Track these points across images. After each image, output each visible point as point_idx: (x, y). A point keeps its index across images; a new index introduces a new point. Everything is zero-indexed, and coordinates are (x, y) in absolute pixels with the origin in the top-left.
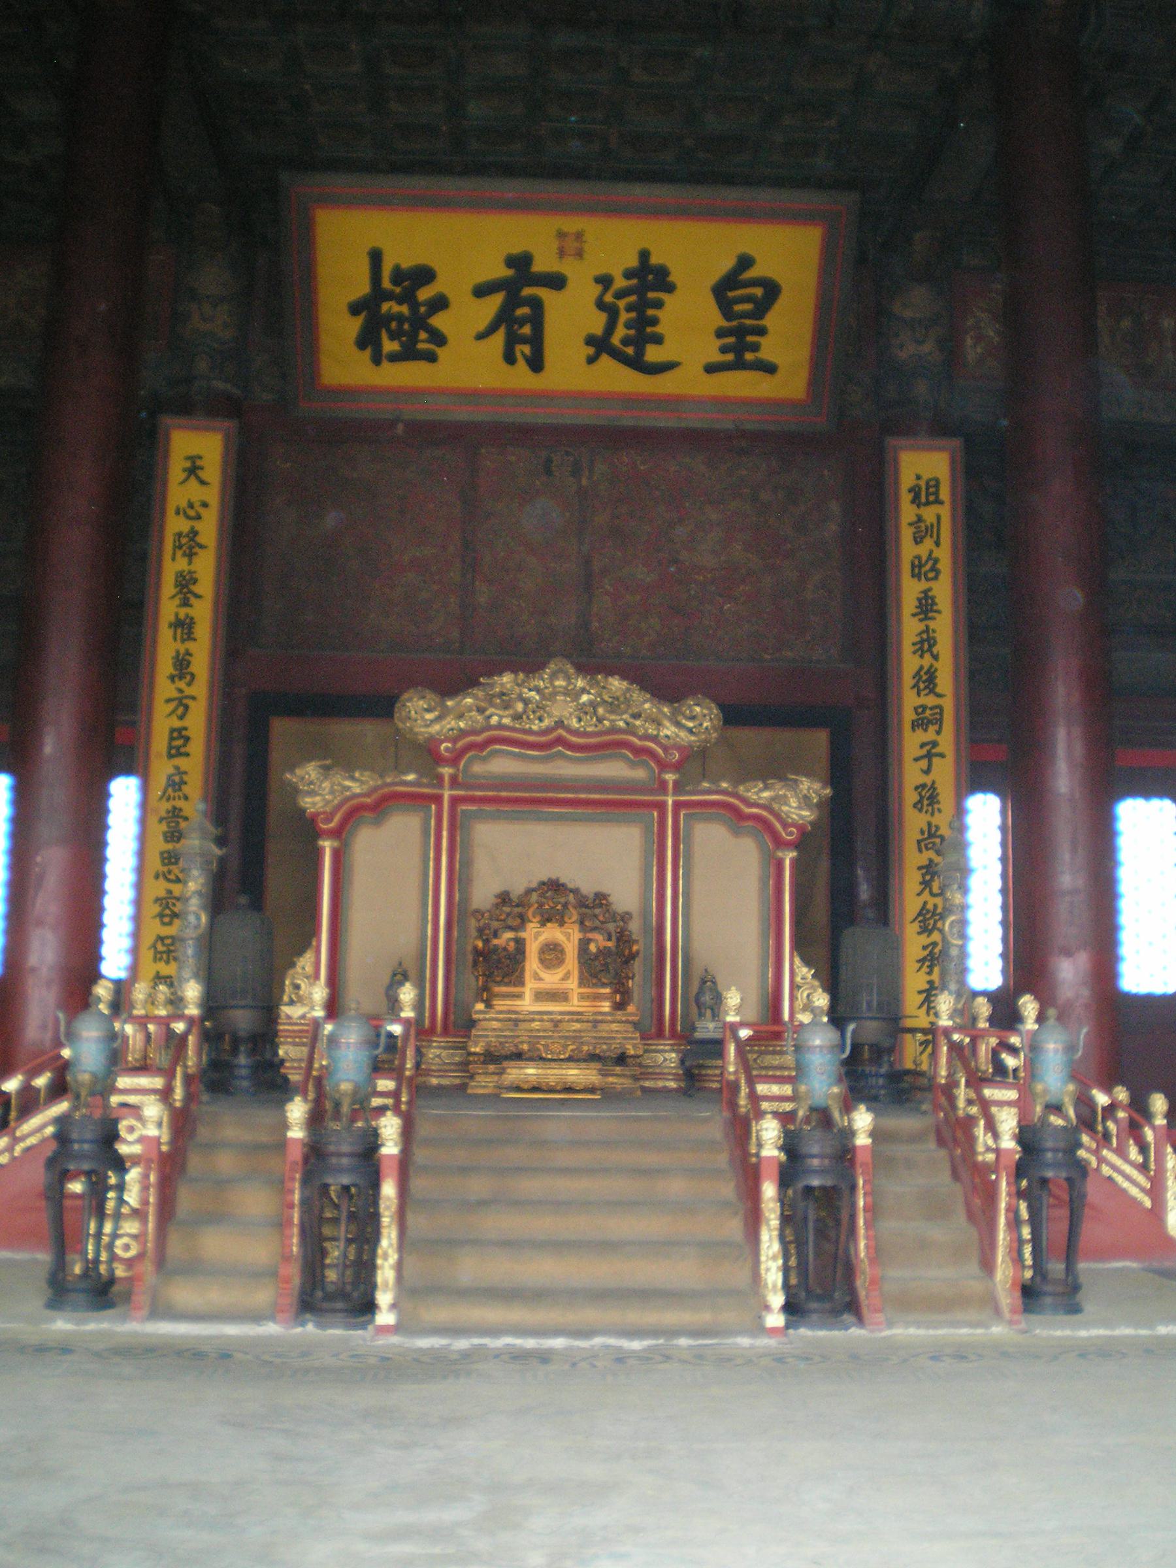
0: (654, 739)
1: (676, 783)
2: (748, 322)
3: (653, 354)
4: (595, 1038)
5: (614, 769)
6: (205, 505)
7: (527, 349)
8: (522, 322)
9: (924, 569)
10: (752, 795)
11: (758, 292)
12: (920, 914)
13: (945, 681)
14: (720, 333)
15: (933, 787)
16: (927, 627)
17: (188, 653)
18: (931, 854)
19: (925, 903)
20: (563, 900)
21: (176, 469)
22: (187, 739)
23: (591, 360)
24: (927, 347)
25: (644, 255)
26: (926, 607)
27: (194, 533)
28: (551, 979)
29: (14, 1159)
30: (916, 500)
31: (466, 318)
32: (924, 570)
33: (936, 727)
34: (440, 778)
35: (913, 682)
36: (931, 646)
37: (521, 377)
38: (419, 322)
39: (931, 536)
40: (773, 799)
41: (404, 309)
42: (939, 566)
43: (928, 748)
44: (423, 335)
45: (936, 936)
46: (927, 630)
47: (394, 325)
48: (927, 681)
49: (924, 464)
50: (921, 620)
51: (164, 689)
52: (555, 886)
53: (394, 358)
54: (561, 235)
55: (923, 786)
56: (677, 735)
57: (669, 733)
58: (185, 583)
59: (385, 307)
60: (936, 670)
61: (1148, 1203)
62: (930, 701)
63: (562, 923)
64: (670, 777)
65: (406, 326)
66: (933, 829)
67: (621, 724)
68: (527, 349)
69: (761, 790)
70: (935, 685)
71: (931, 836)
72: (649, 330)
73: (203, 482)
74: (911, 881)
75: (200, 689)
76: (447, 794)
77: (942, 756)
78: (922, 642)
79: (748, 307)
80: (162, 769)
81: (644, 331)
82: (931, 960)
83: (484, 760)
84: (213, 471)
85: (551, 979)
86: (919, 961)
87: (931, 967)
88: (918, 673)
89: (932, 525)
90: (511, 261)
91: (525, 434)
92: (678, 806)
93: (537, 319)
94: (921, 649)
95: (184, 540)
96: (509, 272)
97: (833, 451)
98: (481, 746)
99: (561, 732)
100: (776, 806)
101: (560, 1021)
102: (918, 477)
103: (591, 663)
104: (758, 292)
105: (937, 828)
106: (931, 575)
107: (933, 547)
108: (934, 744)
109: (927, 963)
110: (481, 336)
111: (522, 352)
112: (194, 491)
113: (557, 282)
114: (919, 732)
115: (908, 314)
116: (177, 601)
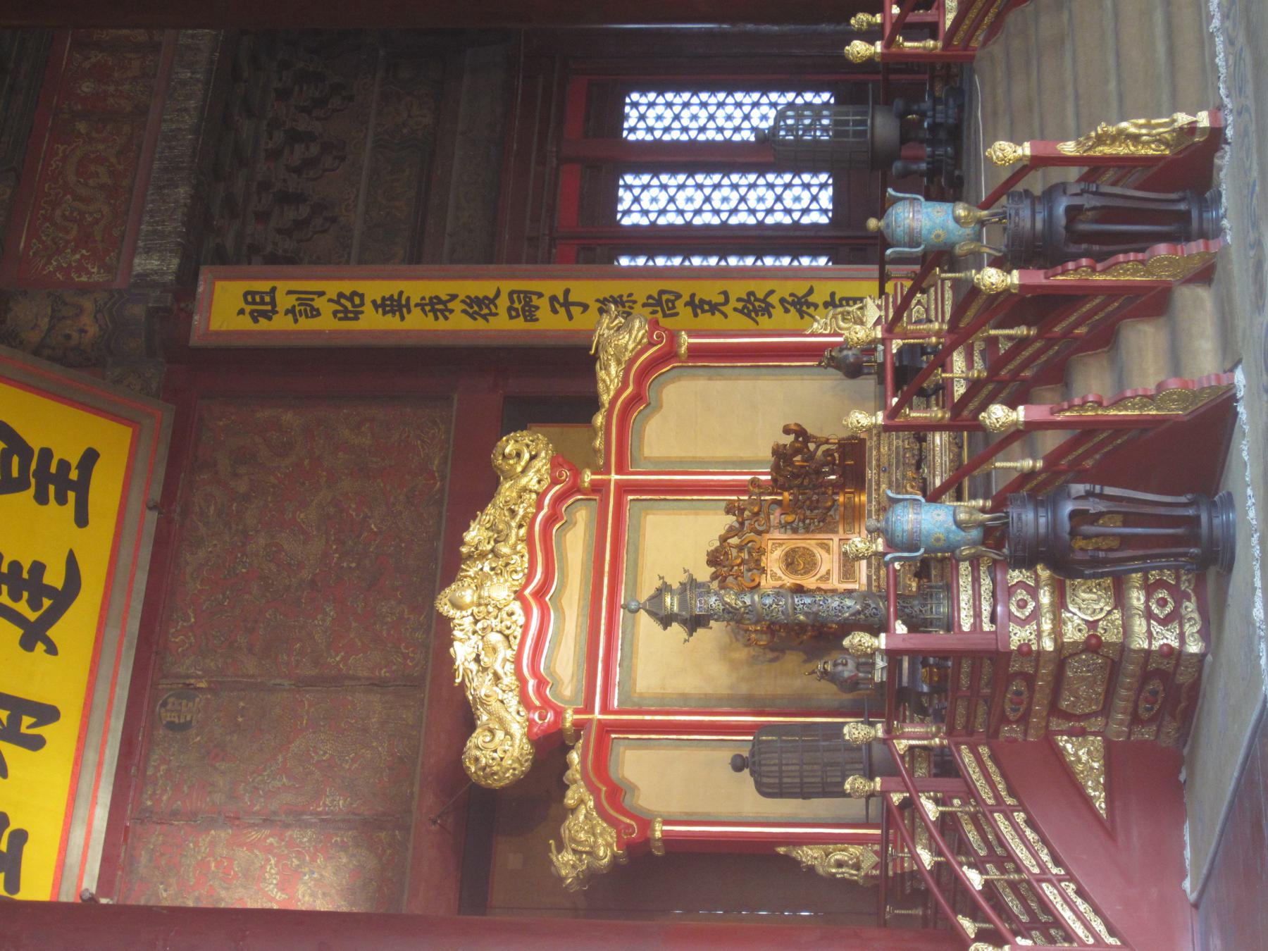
0: (541, 496)
1: (593, 473)
2: (33, 466)
3: (55, 578)
4: (897, 468)
7: (27, 720)
9: (349, 307)
12: (748, 315)
13: (483, 288)
14: (42, 498)
15: (604, 301)
16: (417, 305)
18: (680, 304)
19: (735, 309)
20: (734, 552)
23: (52, 649)
26: (394, 306)
28: (828, 562)
29: (1071, 878)
30: (268, 316)
32: (350, 308)
33: (534, 298)
35: (480, 320)
36: (440, 301)
37: (61, 736)
39: (313, 300)
40: (619, 362)
42: (348, 294)
43: (557, 306)
45: (773, 299)
46: (421, 305)
48: (479, 306)
49: (226, 307)
50: (409, 311)
56: (539, 470)
57: (535, 479)
60: (468, 297)
62: (503, 302)
63: (762, 552)
64: (588, 477)
66: (651, 301)
67: (523, 531)
68: (27, 720)
69: (609, 374)
70: (486, 298)
71: (659, 303)
72: (25, 575)
76: (597, 715)
77: (567, 292)
78: (434, 310)
79: (16, 459)
82: (802, 305)
83: (557, 684)
85: (828, 562)
86: (802, 317)
87: (809, 305)
88: (472, 316)
89: (298, 299)
94: (442, 311)
97: (202, 402)
98: (541, 683)
99: (527, 592)
100: (628, 355)
101: (879, 503)
102: (242, 312)
103: (450, 566)
105: (650, 297)
106: (357, 301)
107: (325, 298)
108: (553, 299)
109: (804, 308)
111: (29, 727)
114: (538, 314)
115: (44, 323)
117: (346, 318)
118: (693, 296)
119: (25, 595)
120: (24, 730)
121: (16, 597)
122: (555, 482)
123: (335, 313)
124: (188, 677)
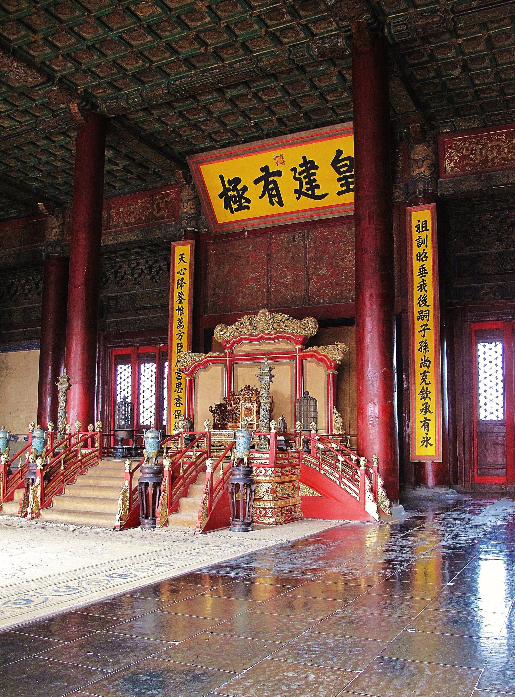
0: (293, 334)
3: (318, 192)
5: (282, 346)
6: (185, 269)
7: (276, 199)
8: (272, 189)
10: (321, 352)
11: (348, 162)
13: (430, 301)
14: (339, 180)
16: (423, 279)
17: (182, 319)
19: (423, 387)
21: (177, 258)
22: (182, 346)
23: (298, 198)
24: (423, 169)
25: (304, 158)
26: (423, 271)
27: (182, 279)
30: (418, 231)
31: (254, 192)
34: (225, 353)
36: (424, 287)
37: (276, 209)
38: (241, 197)
41: (235, 193)
44: (243, 201)
47: (234, 199)
48: (424, 301)
51: (176, 331)
52: (248, 388)
53: (237, 210)
54: (276, 157)
55: (422, 342)
58: (180, 295)
59: (229, 194)
61: (358, 499)
62: (425, 308)
65: (237, 199)
68: (276, 199)
70: (426, 302)
71: (425, 361)
72: (314, 184)
73: (185, 262)
74: (418, 378)
75: (185, 330)
76: (227, 358)
77: (429, 329)
79: (346, 168)
80: (175, 356)
81: (313, 185)
84: (187, 259)
90: (262, 170)
91: (285, 228)
92: (302, 357)
93: (276, 187)
94: (421, 288)
95: (180, 282)
96: (264, 173)
102: (419, 221)
103: (273, 310)
104: (348, 162)
105: (428, 358)
106: (424, 259)
107: (425, 248)
108: (426, 325)
110: (260, 198)
112: (183, 265)
113: (279, 173)
116: (178, 302)
117: (417, 257)
118: (429, 372)
119: (309, 186)
120: (273, 199)
121: (306, 183)
122: (295, 336)
123: (419, 253)
124: (308, 238)
